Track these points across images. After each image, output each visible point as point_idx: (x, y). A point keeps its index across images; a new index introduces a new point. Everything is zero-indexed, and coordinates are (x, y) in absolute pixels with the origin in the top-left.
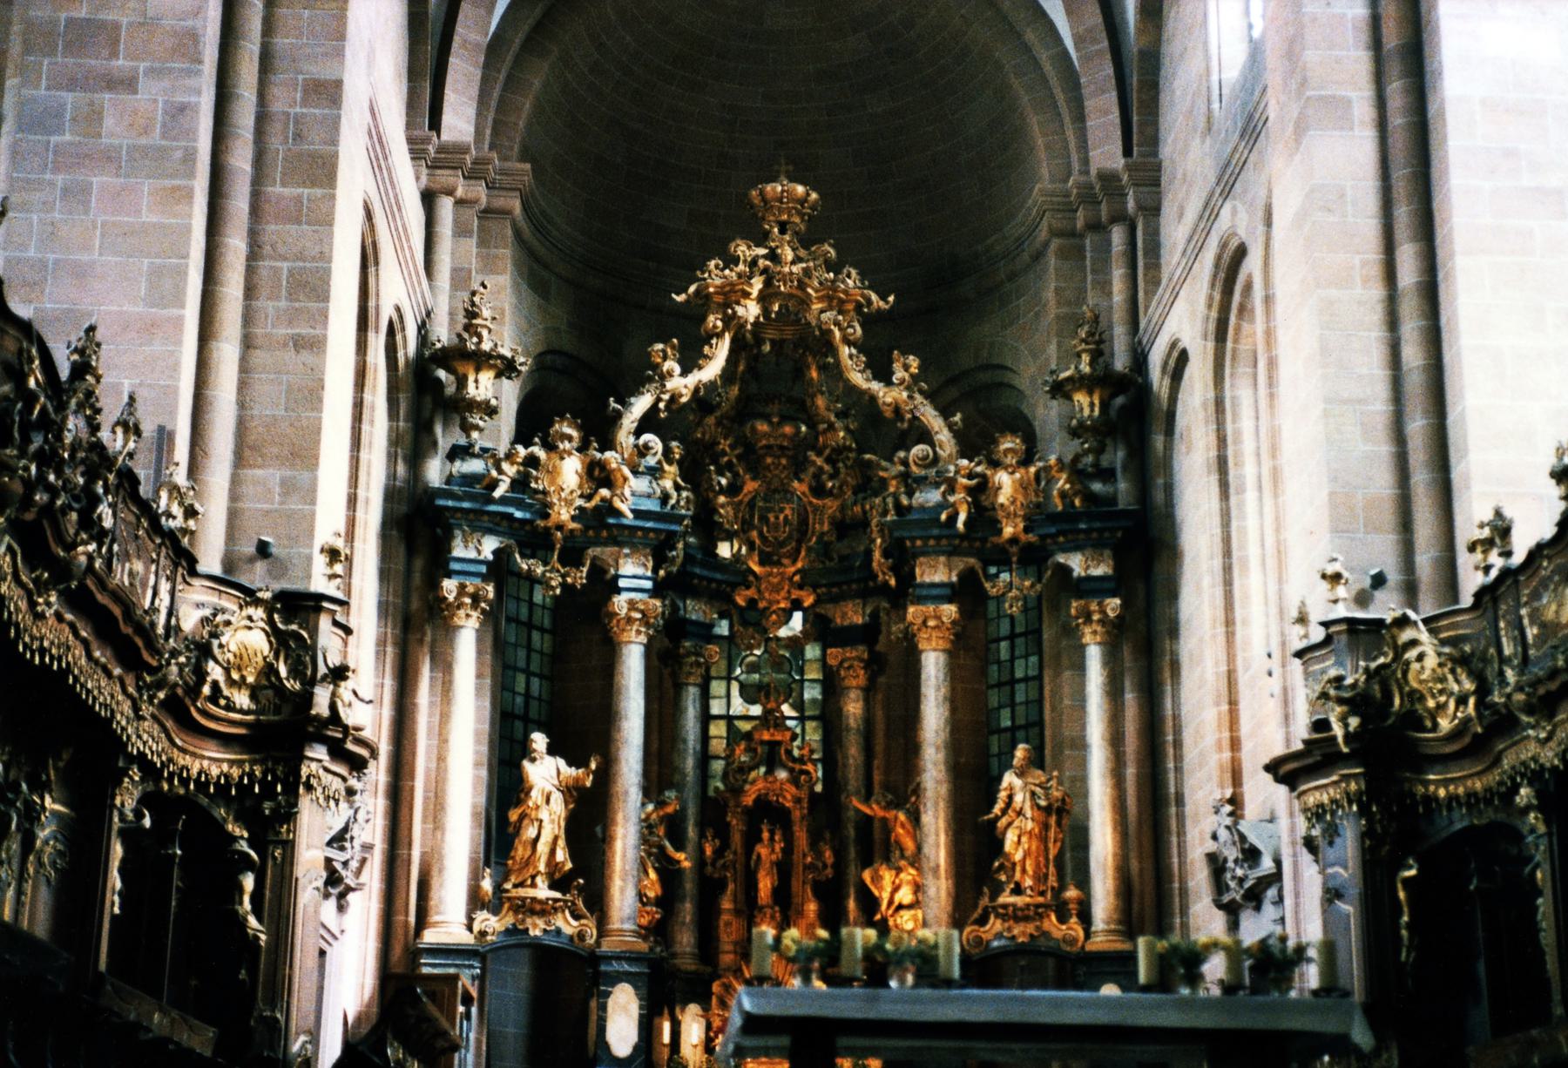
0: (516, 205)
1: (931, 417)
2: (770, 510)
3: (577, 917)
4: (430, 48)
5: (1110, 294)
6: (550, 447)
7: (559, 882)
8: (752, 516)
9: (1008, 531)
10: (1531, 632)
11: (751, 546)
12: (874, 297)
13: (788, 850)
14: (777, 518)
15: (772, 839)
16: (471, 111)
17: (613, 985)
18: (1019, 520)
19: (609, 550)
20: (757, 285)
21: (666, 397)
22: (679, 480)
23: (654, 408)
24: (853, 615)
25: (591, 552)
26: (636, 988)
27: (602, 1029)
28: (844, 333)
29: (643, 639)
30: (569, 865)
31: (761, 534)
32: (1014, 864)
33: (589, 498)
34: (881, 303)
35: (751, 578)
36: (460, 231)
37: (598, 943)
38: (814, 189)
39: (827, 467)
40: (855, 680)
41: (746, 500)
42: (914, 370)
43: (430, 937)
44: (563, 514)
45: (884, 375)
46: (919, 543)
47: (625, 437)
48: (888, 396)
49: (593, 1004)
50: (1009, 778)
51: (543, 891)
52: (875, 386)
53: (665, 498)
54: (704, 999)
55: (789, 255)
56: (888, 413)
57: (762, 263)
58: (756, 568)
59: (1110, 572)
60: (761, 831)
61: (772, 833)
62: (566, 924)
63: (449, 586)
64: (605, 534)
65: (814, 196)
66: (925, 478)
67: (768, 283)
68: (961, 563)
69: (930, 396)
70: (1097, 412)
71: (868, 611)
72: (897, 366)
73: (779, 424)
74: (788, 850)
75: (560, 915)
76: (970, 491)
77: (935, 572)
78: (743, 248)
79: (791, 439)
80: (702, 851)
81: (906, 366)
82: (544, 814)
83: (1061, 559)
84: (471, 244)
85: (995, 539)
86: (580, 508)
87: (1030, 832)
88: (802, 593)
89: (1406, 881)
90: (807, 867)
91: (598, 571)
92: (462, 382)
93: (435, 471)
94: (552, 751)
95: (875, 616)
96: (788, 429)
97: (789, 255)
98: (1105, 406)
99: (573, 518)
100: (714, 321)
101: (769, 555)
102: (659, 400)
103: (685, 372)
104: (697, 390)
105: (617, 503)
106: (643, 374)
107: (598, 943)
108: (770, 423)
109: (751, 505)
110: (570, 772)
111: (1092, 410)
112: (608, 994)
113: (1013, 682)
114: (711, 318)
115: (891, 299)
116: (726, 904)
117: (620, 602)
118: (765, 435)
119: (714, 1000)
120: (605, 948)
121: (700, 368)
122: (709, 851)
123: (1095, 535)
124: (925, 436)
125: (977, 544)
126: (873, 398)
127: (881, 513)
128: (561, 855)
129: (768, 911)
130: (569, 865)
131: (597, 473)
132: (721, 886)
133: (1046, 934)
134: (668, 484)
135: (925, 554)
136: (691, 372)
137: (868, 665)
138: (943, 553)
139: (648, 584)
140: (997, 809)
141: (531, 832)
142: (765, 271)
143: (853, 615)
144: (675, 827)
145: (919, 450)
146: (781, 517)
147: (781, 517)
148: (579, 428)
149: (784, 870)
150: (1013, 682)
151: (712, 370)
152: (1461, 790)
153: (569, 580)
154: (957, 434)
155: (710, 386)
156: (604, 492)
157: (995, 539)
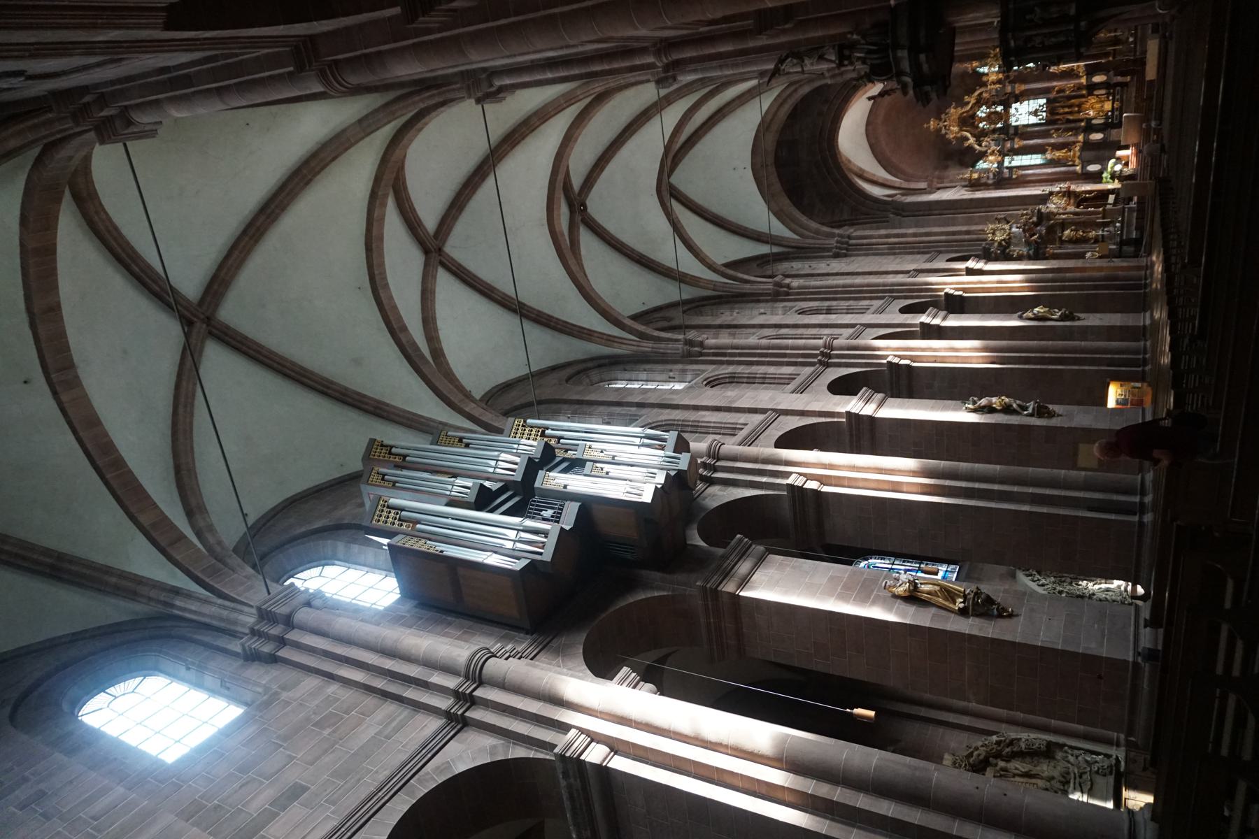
0: (937, 173)
1: (977, 93)
4: (912, 192)
16: (919, 184)
20: (952, 128)
28: (960, 111)
36: (942, 183)
42: (966, 97)
43: (1080, 172)
45: (968, 103)
47: (984, 149)
48: (973, 101)
52: (970, 105)
53: (993, 140)
62: (1078, 148)
63: (1014, 176)
68: (1007, 84)
69: (972, 94)
72: (967, 100)
77: (1009, 89)
84: (945, 180)
92: (975, 179)
93: (990, 182)
100: (959, 135)
106: (970, 148)
116: (1071, 118)
127: (996, 100)
132: (1068, 119)
144: (1057, 130)
149: (1063, 107)
151: (968, 135)
154: (981, 87)
155: (971, 134)
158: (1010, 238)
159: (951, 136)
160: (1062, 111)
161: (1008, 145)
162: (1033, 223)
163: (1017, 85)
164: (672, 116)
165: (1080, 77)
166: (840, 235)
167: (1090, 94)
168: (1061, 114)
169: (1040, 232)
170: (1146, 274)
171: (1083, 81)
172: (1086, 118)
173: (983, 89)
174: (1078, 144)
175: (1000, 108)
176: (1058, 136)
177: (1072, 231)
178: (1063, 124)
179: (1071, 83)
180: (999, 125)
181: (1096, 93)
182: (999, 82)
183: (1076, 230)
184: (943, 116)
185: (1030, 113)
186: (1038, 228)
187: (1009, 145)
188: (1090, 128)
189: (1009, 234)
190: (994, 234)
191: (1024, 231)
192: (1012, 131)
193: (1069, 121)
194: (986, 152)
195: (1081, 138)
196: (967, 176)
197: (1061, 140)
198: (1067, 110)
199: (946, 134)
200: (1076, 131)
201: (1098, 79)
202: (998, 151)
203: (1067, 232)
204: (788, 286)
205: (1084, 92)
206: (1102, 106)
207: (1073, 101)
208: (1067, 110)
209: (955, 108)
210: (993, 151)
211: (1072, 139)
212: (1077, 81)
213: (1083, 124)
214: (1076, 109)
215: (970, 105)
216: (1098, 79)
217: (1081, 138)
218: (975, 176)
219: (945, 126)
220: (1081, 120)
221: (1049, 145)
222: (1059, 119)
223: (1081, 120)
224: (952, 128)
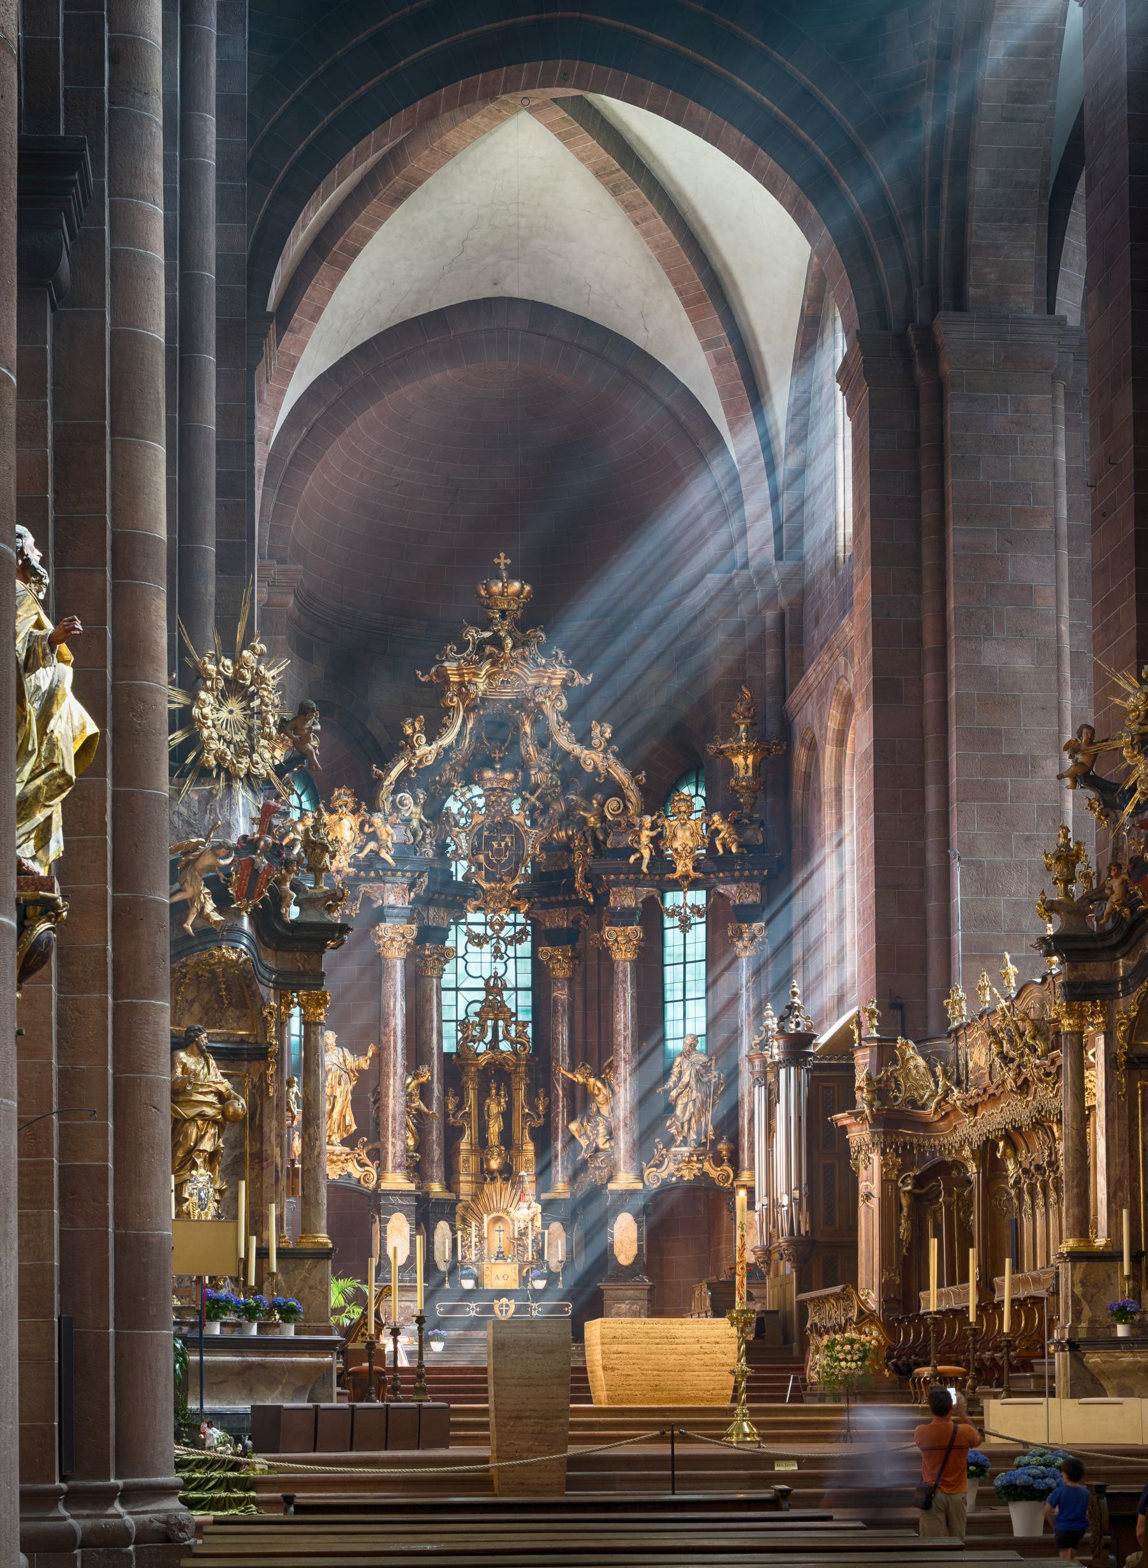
1: (620, 773)
2: (495, 839)
3: (362, 1165)
5: (763, 668)
6: (332, 811)
7: (349, 1142)
8: (480, 844)
9: (680, 869)
10: (971, 1065)
11: (479, 867)
12: (576, 673)
13: (510, 1104)
14: (500, 845)
15: (498, 1094)
17: (390, 1214)
18: (687, 861)
19: (376, 885)
21: (415, 762)
22: (422, 817)
23: (405, 772)
24: (559, 920)
25: (363, 888)
26: (407, 1216)
27: (383, 1247)
29: (403, 955)
30: (354, 1127)
31: (487, 857)
32: (682, 1124)
33: (361, 849)
34: (582, 680)
35: (480, 892)
37: (378, 1185)
38: (527, 582)
39: (538, 804)
40: (561, 971)
41: (475, 830)
42: (608, 735)
45: (584, 739)
46: (612, 877)
47: (385, 795)
48: (591, 758)
49: (376, 1227)
52: (577, 749)
54: (450, 1217)
55: (509, 642)
56: (589, 769)
57: (489, 649)
58: (485, 885)
59: (758, 901)
60: (490, 1089)
61: (498, 1090)
62: (357, 1172)
64: (372, 874)
65: (527, 588)
66: (619, 824)
67: (493, 664)
68: (644, 891)
70: (750, 771)
71: (571, 918)
72: (596, 732)
73: (502, 770)
74: (510, 1104)
75: (350, 1164)
76: (654, 840)
78: (473, 632)
79: (511, 782)
80: (446, 1105)
81: (602, 732)
82: (338, 1092)
83: (721, 889)
85: (671, 876)
86: (354, 856)
87: (694, 1101)
88: (518, 903)
89: (909, 1192)
90: (525, 1116)
91: (367, 900)
94: (339, 1044)
95: (576, 922)
96: (508, 776)
97: (509, 642)
98: (756, 767)
99: (350, 865)
101: (493, 874)
102: (410, 764)
103: (429, 743)
104: (438, 754)
105: (384, 854)
106: (398, 745)
107: (378, 1185)
108: (494, 769)
109: (479, 834)
110: (349, 1058)
111: (747, 772)
112: (387, 1221)
114: (449, 694)
115: (590, 678)
116: (464, 1145)
117: (386, 929)
118: (490, 779)
119: (458, 1217)
120: (384, 1186)
121: (440, 735)
122: (450, 1107)
123: (747, 873)
125: (657, 877)
126: (577, 758)
128: (350, 1118)
129: (496, 1150)
130: (354, 1127)
131: (367, 827)
132: (460, 1131)
133: (705, 1174)
134: (415, 823)
135: (617, 884)
136: (434, 740)
137: (572, 959)
138: (631, 884)
139: (408, 912)
140: (671, 1083)
142: (491, 655)
143: (559, 920)
144: (424, 1091)
145: (613, 803)
146: (503, 844)
147: (503, 844)
148: (354, 795)
152: (937, 1143)
153: (347, 912)
155: (450, 747)
156: (372, 845)
157: (671, 876)
158: (204, 773)
159: (450, 666)
160: (494, 1108)
161: (394, 897)
162: (278, 901)
163: (635, 931)
168: (481, 1105)
169: (231, 933)
170: (166, 1491)
171: (624, 1180)
172: (453, 1204)
173: (633, 795)
177: (222, 1097)
178: (446, 1115)
180: (460, 869)
183: (221, 1124)
185: (494, 987)
186: (246, 924)
187: (391, 899)
189: (231, 777)
190: (234, 687)
191: (248, 844)
192: (434, 916)
193: (452, 1135)
194: (373, 808)
195: (397, 1180)
197: (394, 1104)
198: (495, 1128)
199: (463, 646)
202: (375, 854)
203: (214, 1076)
205: (560, 1187)
206: (500, 1256)
207: (530, 1147)
208: (495, 1128)
210: (373, 836)
213: (436, 1188)
214: (494, 1164)
215: (577, 749)
219: (497, 641)
220: (450, 1183)
221: (379, 1060)
222: (461, 1093)
223: (450, 1183)
224: (487, 667)
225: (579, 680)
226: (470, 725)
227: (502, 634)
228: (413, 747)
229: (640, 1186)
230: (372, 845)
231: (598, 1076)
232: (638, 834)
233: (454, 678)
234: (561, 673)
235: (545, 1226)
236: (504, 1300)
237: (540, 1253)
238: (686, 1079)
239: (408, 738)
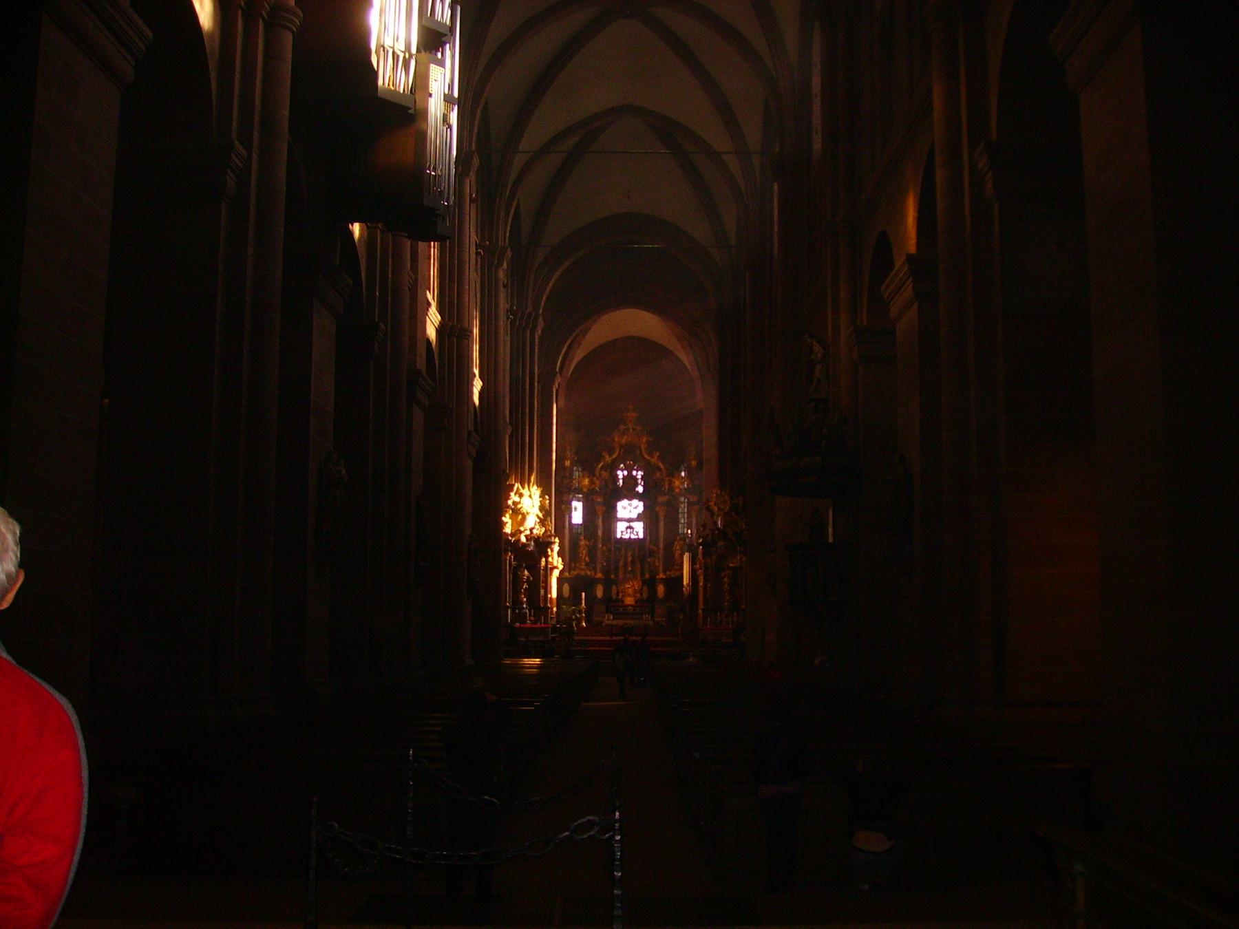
3: (590, 570)
7: (587, 564)
42: (658, 454)
44: (585, 490)
45: (652, 457)
47: (597, 473)
48: (653, 460)
50: (676, 543)
51: (583, 567)
62: (589, 573)
63: (563, 507)
68: (666, 497)
72: (654, 453)
110: (588, 543)
113: (684, 513)
124: (660, 470)
128: (587, 559)
134: (607, 478)
141: (581, 555)
145: (658, 474)
150: (684, 513)
151: (614, 456)
156: (593, 486)
164: (718, 139)
165: (665, 573)
166: (537, 316)
167: (644, 582)
171: (661, 576)
174: (593, 572)
175: (640, 489)
176: (603, 552)
179: (660, 565)
181: (645, 588)
182: (671, 488)
184: (639, 428)
187: (599, 500)
188: (608, 583)
194: (594, 476)
195: (599, 575)
196: (568, 454)
197: (599, 554)
200: (606, 572)
201: (661, 589)
202: (594, 489)
204: (500, 265)
206: (629, 595)
208: (630, 559)
209: (647, 441)
210: (594, 483)
211: (599, 567)
212: (661, 569)
213: (613, 576)
214: (630, 569)
216: (661, 589)
217: (599, 575)
218: (568, 463)
219: (628, 429)
220: (617, 576)
225: (650, 439)
226: (622, 451)
227: (630, 427)
228: (605, 459)
229: (664, 577)
230: (593, 486)
231: (655, 546)
232: (664, 482)
233: (616, 439)
234: (645, 439)
235: (642, 586)
236: (630, 607)
237: (641, 594)
238: (678, 547)
239: (604, 456)
